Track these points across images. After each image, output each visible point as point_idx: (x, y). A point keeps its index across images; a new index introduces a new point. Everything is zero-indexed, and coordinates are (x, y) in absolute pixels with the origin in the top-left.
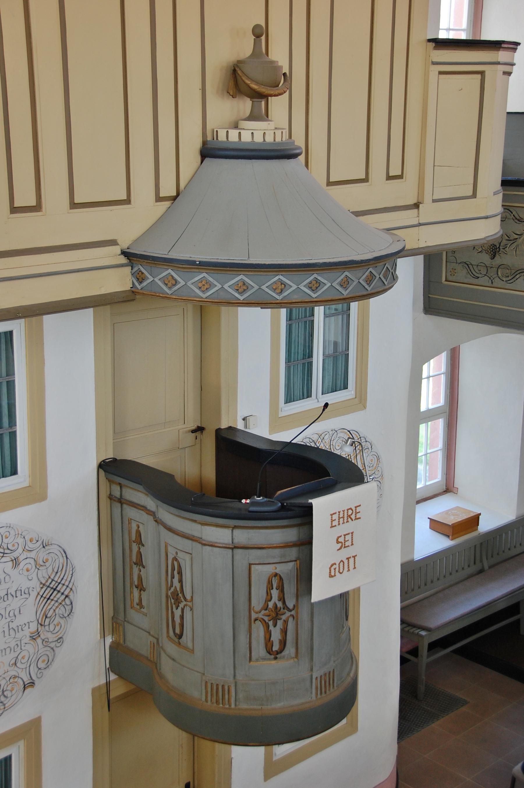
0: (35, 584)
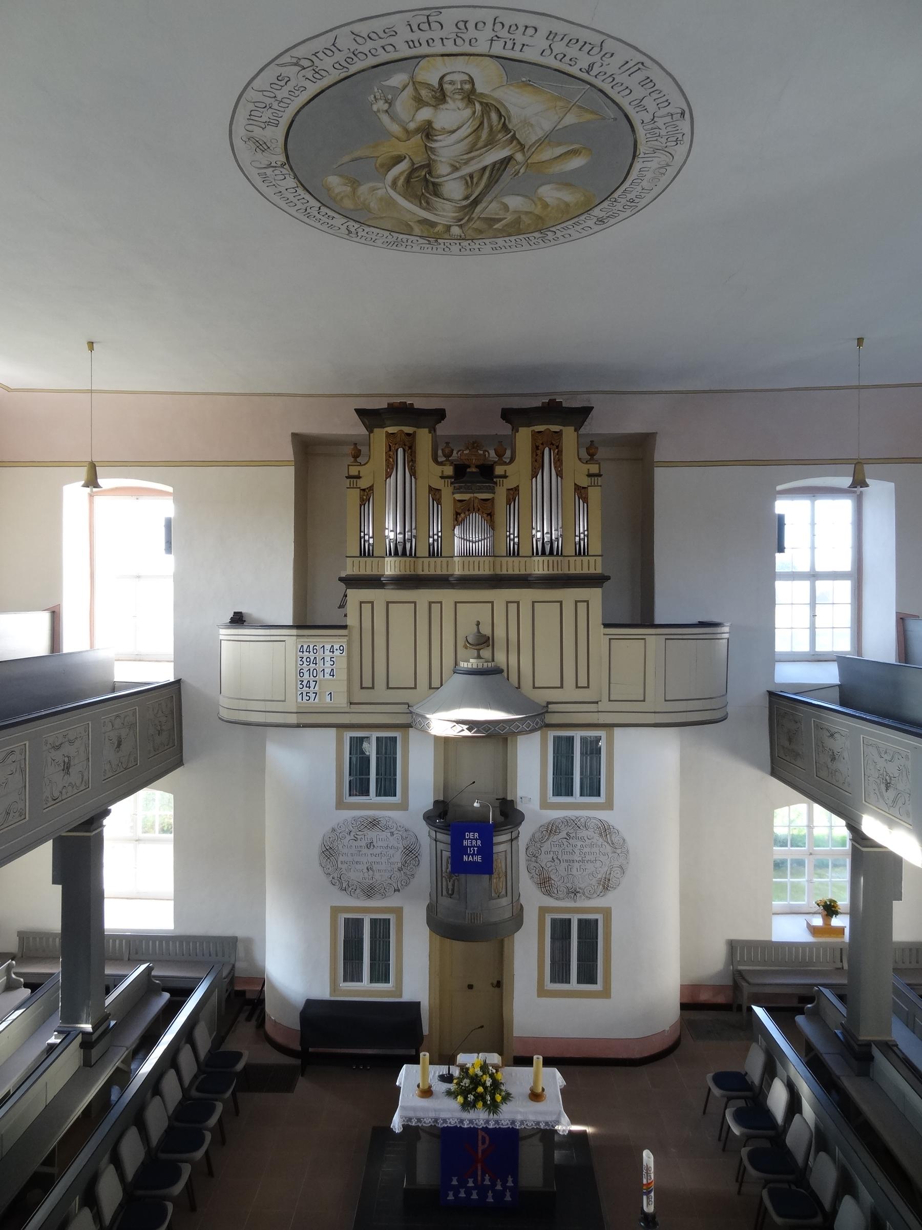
0: (400, 846)
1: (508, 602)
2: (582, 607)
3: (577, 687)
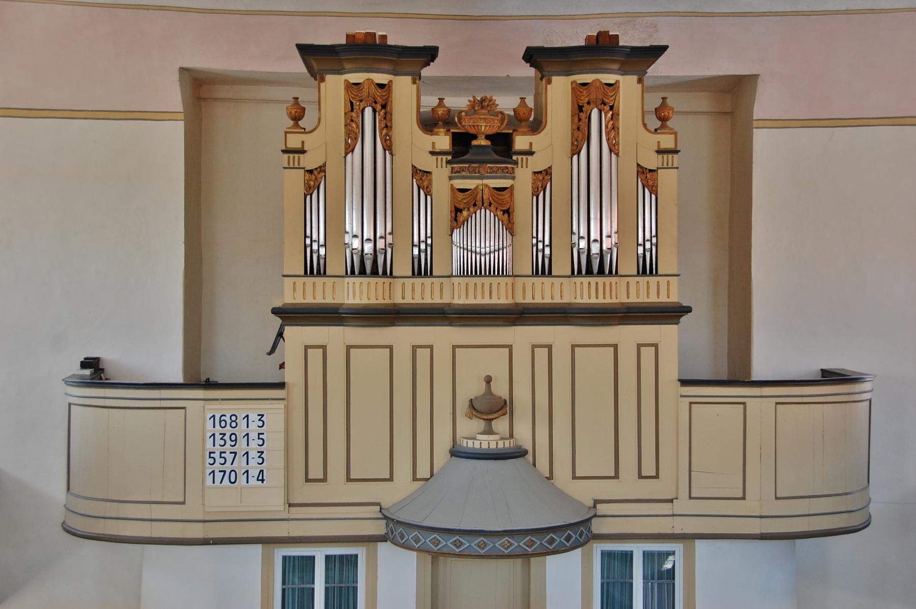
1: (534, 347)
2: (648, 354)
3: (641, 477)
